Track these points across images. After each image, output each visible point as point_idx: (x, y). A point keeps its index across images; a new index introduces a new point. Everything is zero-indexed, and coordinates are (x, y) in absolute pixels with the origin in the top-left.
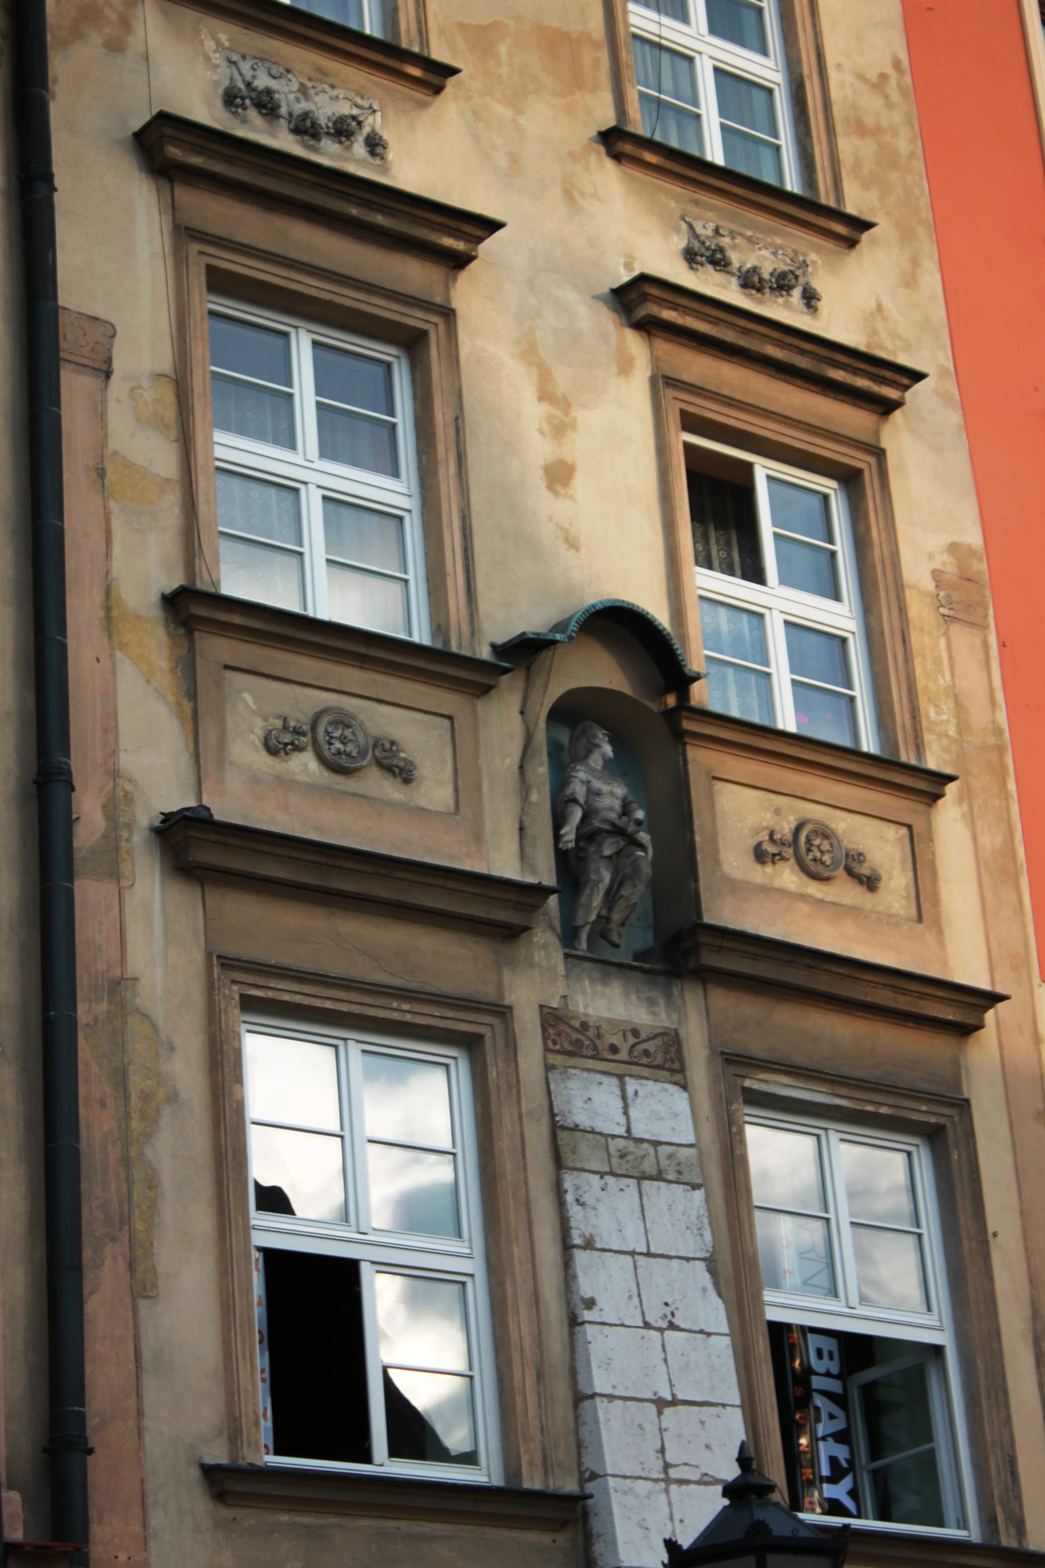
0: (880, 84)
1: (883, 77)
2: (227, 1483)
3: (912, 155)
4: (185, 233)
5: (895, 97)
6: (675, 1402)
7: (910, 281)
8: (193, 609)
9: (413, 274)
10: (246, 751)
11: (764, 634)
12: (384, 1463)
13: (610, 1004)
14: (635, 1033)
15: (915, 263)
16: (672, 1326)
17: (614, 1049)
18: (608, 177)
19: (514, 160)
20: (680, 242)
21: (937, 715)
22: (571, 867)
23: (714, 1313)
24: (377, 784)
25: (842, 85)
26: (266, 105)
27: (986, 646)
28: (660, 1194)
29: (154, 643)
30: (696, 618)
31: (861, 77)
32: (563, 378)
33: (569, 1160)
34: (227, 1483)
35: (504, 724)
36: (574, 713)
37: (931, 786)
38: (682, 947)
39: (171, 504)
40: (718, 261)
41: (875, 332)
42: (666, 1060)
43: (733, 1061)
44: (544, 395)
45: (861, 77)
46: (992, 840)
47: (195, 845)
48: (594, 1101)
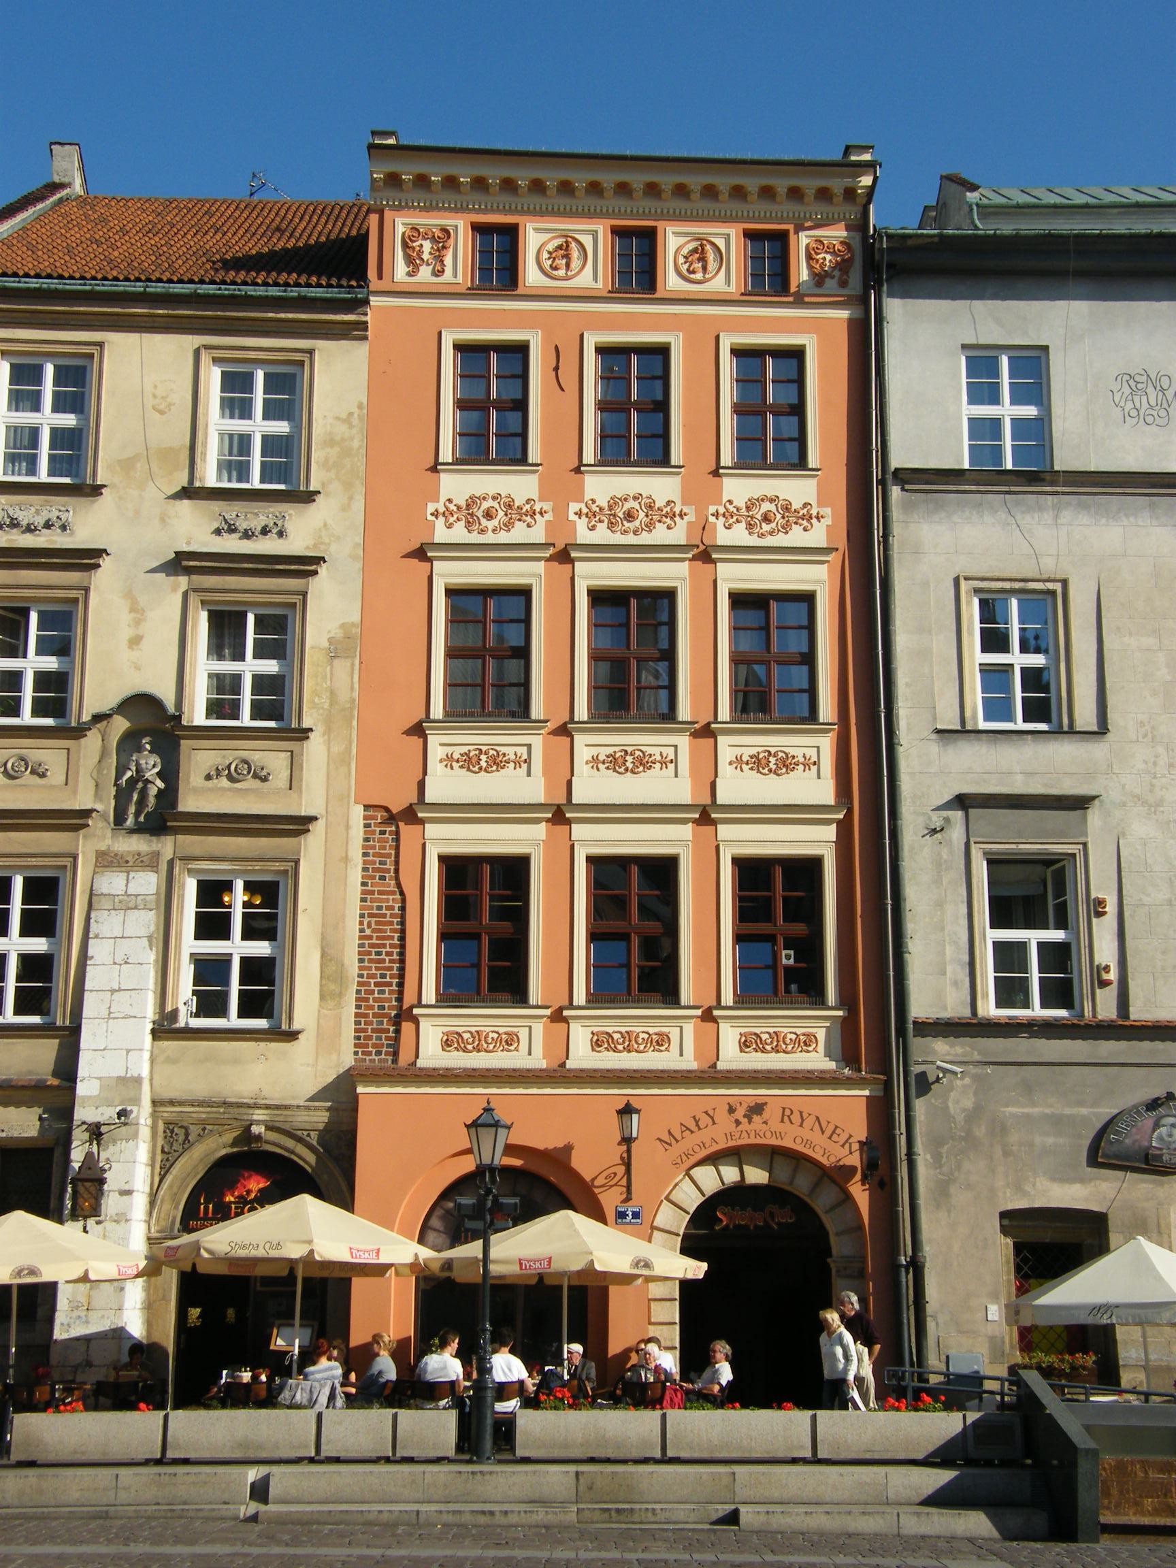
1: (351, 414)
3: (360, 447)
5: (355, 421)
6: (120, 990)
7: (345, 508)
14: (139, 854)
15: (351, 498)
16: (126, 963)
17: (127, 862)
19: (137, 512)
20: (216, 525)
22: (122, 797)
27: (353, 665)
28: (133, 914)
31: (338, 418)
32: (143, 600)
33: (95, 905)
41: (320, 537)
44: (133, 610)
45: (338, 418)
46: (337, 748)
48: (113, 883)
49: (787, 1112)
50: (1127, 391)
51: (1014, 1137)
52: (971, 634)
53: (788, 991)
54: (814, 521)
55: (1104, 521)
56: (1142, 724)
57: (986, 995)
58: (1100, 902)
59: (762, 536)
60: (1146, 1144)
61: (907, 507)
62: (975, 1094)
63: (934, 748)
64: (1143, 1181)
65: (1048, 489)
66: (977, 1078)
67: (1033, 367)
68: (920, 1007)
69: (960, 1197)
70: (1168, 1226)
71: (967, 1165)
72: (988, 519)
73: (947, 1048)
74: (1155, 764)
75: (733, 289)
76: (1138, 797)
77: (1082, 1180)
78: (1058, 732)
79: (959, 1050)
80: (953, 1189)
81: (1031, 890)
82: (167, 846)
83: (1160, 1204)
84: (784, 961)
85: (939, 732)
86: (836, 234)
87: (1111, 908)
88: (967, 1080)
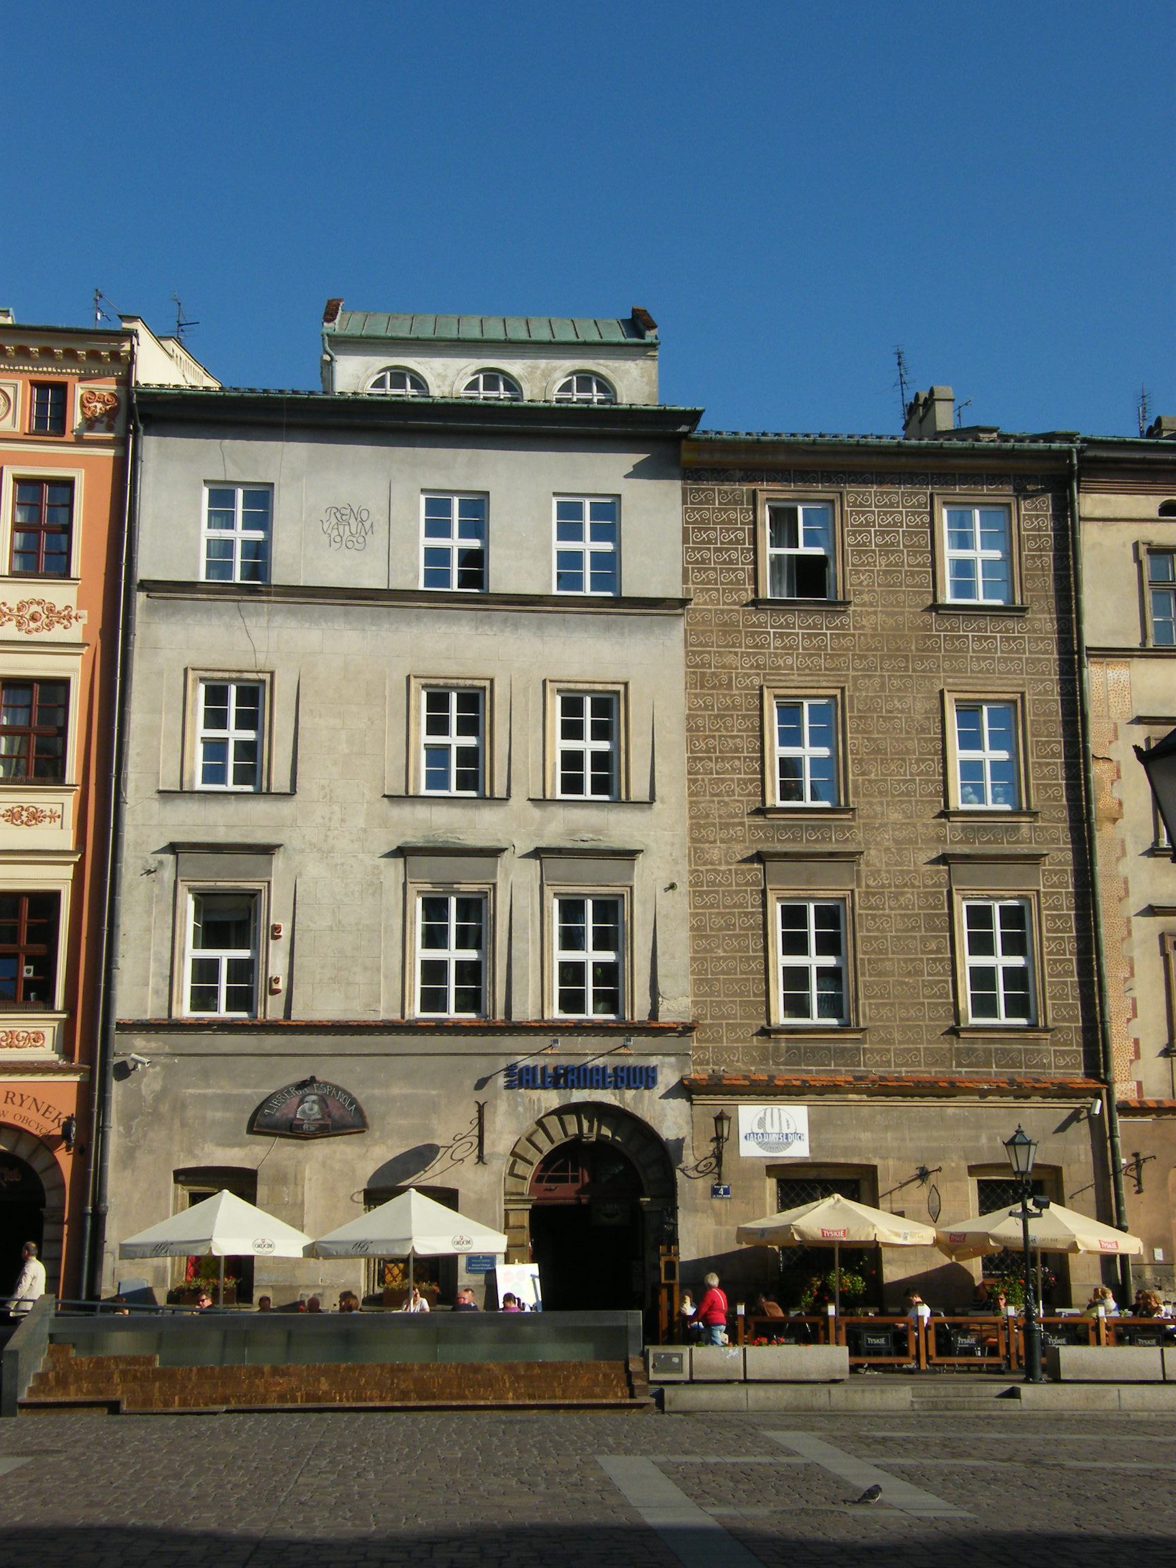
49: (11, 1095)
50: (334, 521)
51: (191, 1112)
52: (194, 714)
53: (27, 998)
54: (73, 621)
55: (307, 625)
56: (323, 787)
57: (181, 1001)
58: (277, 928)
59: (29, 632)
60: (291, 1116)
61: (150, 611)
62: (163, 1080)
63: (156, 806)
64: (289, 1145)
65: (264, 598)
66: (166, 1067)
67: (261, 501)
68: (124, 1010)
69: (143, 1159)
70: (303, 1179)
71: (151, 1135)
72: (215, 621)
73: (144, 1043)
74: (330, 819)
75: (17, 429)
76: (313, 845)
77: (241, 1145)
78: (258, 793)
79: (153, 1045)
80: (138, 1154)
81: (229, 919)
83: (299, 1162)
84: (25, 975)
85: (160, 792)
86: (107, 387)
87: (285, 933)
88: (158, 1069)
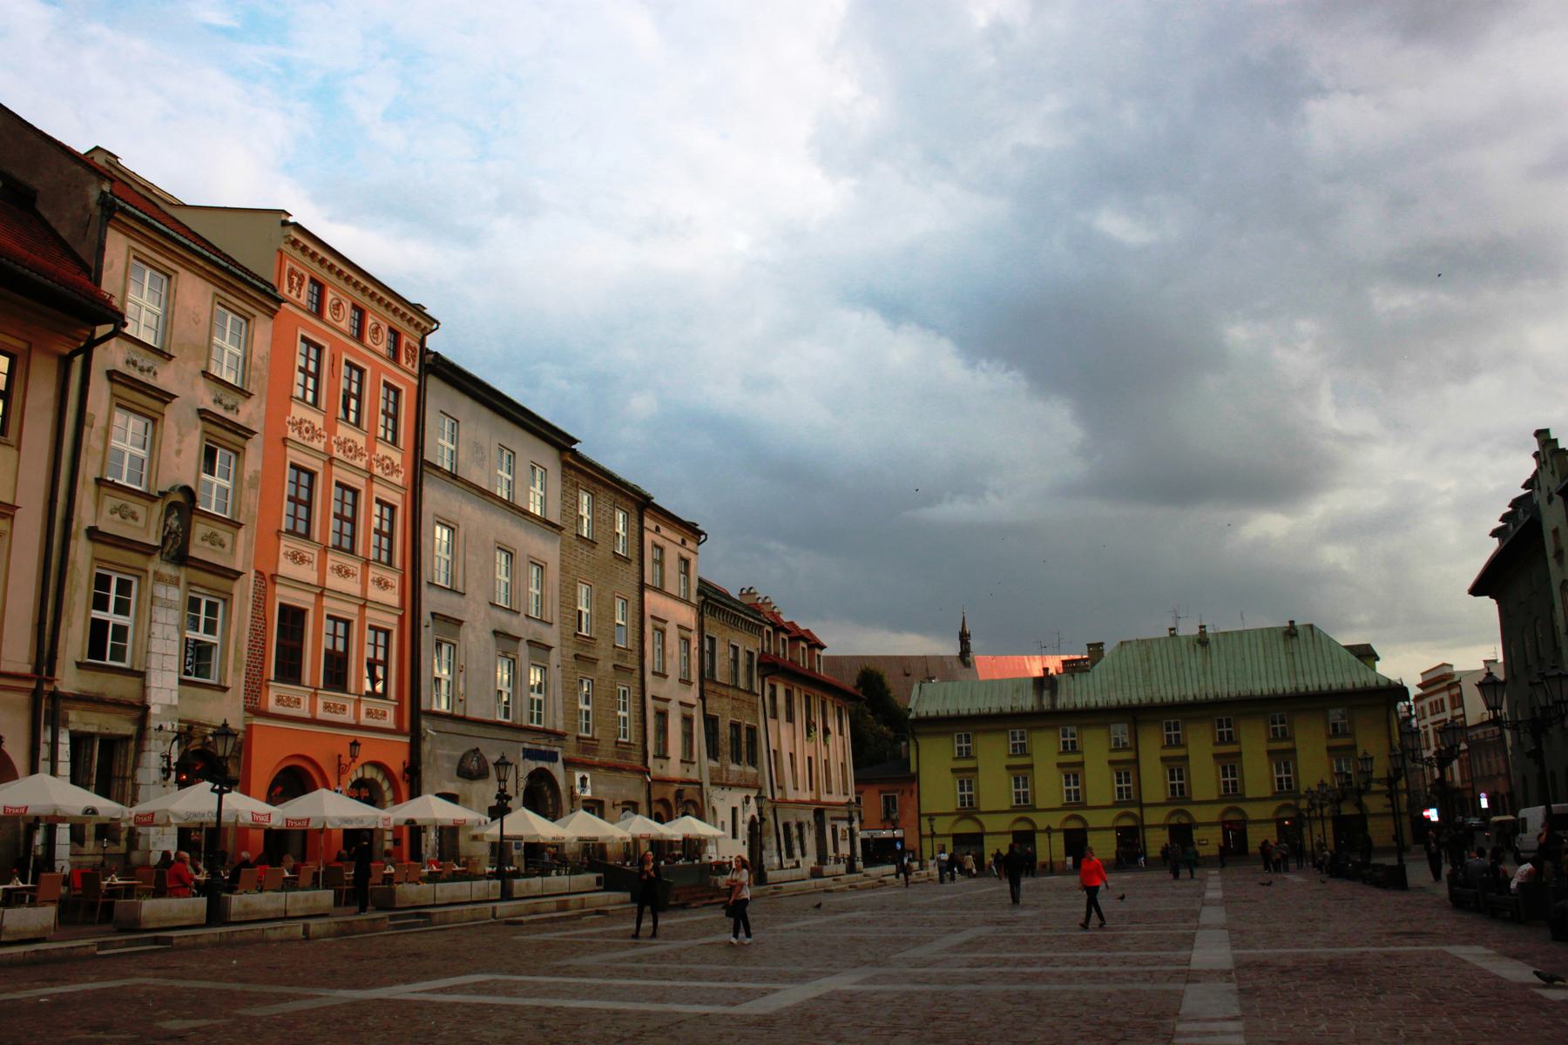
0: (262, 358)
2: (79, 665)
4: (113, 395)
8: (100, 482)
9: (156, 405)
10: (106, 513)
11: (214, 490)
12: (108, 662)
13: (168, 570)
18: (201, 381)
21: (244, 509)
23: (176, 637)
24: (130, 521)
25: (255, 358)
26: (134, 364)
29: (92, 487)
30: (201, 484)
34: (79, 665)
35: (158, 508)
36: (173, 506)
37: (240, 526)
38: (181, 558)
39: (100, 457)
40: (220, 402)
42: (175, 582)
43: (190, 583)
47: (93, 534)
48: (161, 591)
82: (183, 574)
